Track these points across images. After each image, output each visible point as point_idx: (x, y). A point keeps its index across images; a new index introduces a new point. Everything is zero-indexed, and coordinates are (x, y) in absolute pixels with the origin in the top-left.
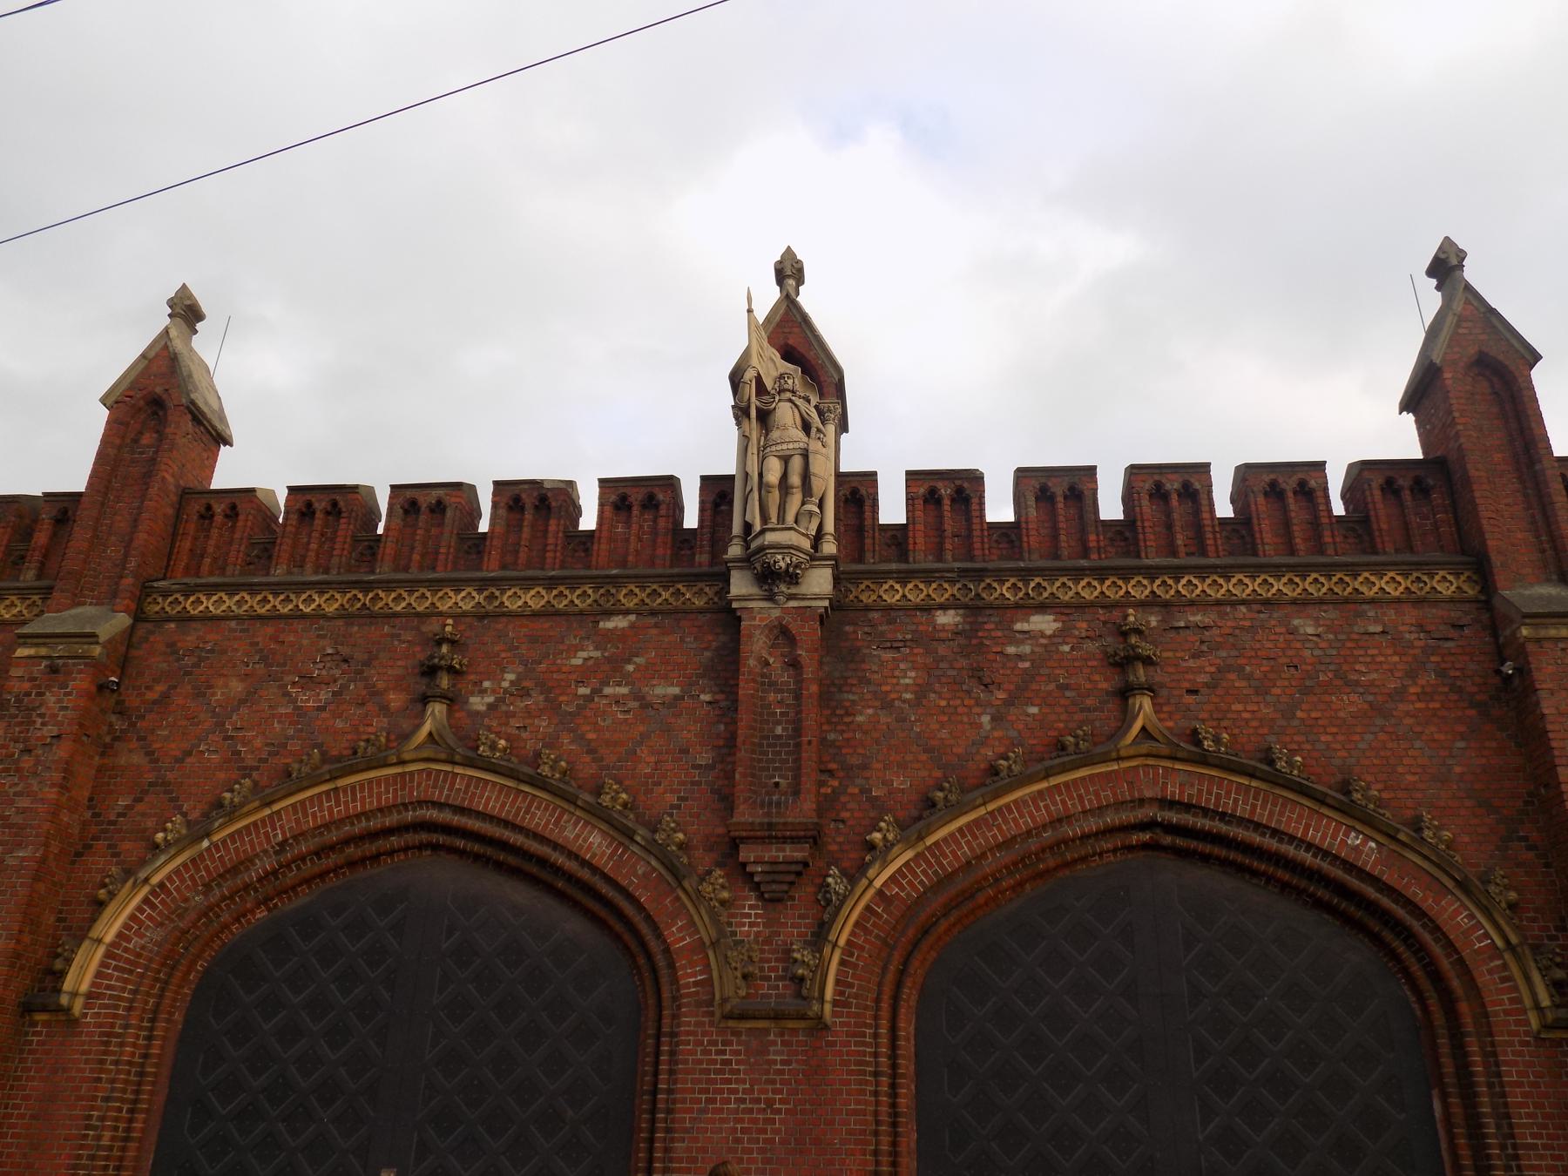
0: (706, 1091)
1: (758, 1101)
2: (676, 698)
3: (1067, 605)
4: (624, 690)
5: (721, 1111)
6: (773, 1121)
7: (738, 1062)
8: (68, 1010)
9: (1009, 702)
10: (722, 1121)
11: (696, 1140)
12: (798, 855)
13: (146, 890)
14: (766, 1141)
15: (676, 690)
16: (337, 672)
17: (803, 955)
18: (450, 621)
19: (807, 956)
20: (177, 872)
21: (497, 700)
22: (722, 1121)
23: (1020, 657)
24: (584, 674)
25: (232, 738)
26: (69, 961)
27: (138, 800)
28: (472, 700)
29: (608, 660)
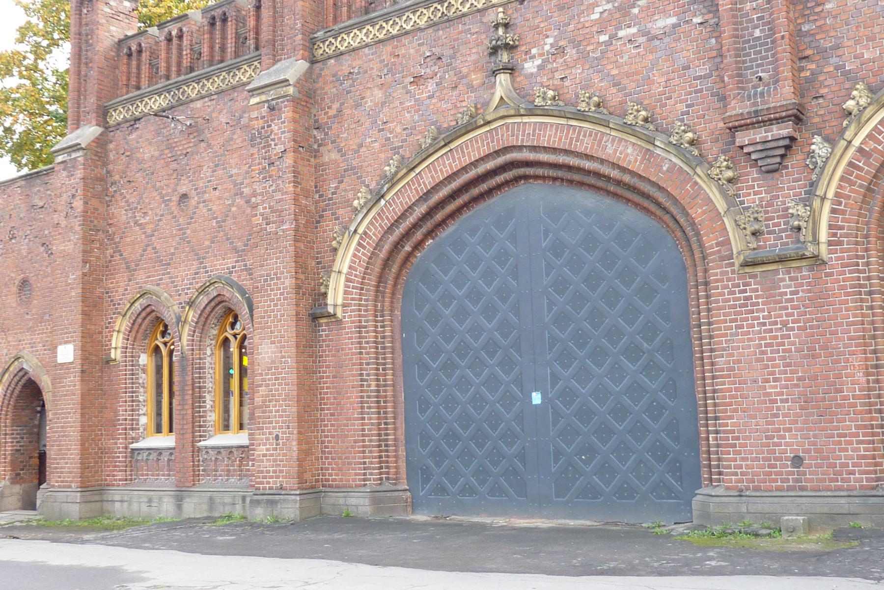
0: (736, 320)
1: (776, 323)
2: (674, 26)
4: (634, 30)
5: (748, 333)
6: (789, 337)
7: (757, 297)
10: (749, 340)
11: (732, 355)
12: (785, 132)
13: (357, 237)
14: (784, 351)
15: (673, 20)
16: (436, 69)
17: (797, 210)
18: (501, 9)
19: (801, 210)
20: (371, 223)
21: (544, 61)
22: (749, 340)
24: (602, 25)
25: (383, 130)
26: (327, 286)
27: (341, 182)
28: (526, 65)
29: (619, 9)
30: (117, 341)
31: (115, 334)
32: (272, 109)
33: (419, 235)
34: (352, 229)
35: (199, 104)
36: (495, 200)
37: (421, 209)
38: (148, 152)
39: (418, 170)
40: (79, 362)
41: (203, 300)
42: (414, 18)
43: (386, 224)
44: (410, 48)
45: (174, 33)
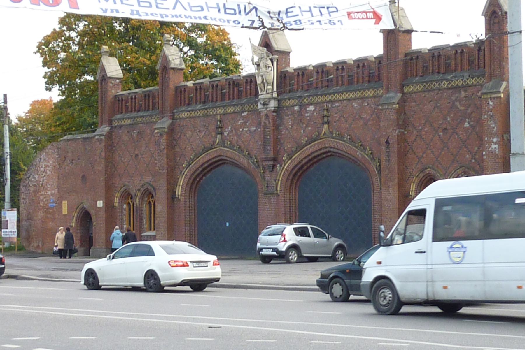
2: (255, 130)
3: (315, 103)
4: (247, 129)
8: (178, 198)
9: (306, 127)
13: (184, 176)
15: (254, 128)
21: (229, 133)
23: (308, 116)
24: (241, 126)
30: (116, 200)
31: (116, 198)
32: (161, 135)
33: (201, 176)
34: (183, 173)
35: (141, 125)
36: (219, 168)
37: (200, 169)
38: (126, 138)
39: (200, 158)
40: (104, 207)
41: (142, 189)
42: (199, 113)
43: (192, 172)
44: (198, 121)
45: (133, 97)
